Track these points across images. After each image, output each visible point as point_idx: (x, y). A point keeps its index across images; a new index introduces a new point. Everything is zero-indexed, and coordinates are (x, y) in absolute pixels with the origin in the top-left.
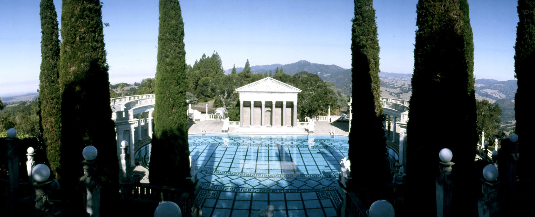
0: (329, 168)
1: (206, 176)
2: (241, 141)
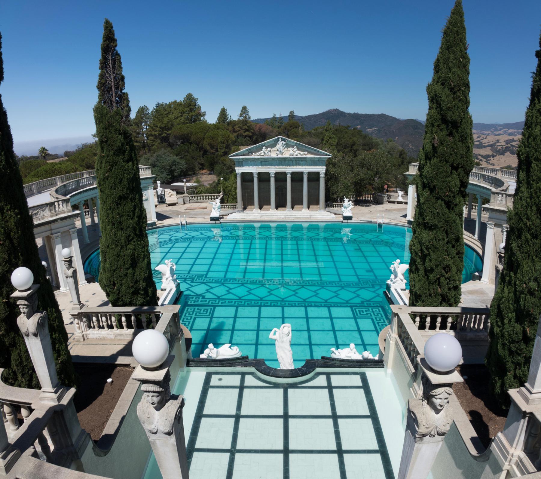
0: (371, 274)
1: (192, 286)
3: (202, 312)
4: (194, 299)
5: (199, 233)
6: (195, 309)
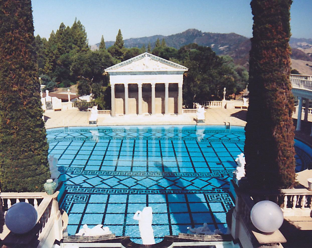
0: (221, 166)
1: (72, 177)
2: (113, 134)
3: (79, 199)
4: (73, 188)
5: (80, 134)
6: (73, 196)
